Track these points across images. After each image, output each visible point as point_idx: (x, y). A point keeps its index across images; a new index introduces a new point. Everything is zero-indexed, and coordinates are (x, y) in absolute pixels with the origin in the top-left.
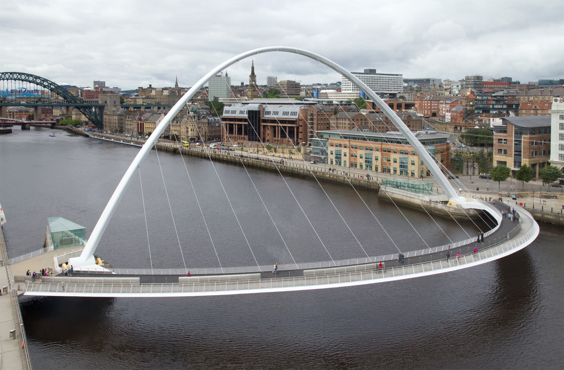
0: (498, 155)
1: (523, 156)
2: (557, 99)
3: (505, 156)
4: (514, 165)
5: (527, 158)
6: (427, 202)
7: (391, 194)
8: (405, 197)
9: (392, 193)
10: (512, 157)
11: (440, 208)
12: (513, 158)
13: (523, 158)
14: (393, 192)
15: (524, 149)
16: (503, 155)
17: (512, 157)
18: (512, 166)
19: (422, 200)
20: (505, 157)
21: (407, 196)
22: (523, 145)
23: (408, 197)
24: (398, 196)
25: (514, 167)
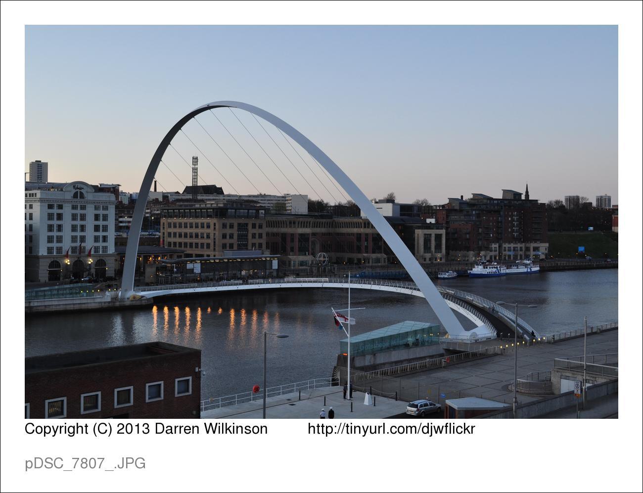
6: (109, 302)
7: (43, 308)
8: (72, 306)
9: (45, 306)
11: (127, 305)
14: (46, 304)
19: (99, 303)
21: (74, 304)
23: (76, 304)
24: (58, 307)
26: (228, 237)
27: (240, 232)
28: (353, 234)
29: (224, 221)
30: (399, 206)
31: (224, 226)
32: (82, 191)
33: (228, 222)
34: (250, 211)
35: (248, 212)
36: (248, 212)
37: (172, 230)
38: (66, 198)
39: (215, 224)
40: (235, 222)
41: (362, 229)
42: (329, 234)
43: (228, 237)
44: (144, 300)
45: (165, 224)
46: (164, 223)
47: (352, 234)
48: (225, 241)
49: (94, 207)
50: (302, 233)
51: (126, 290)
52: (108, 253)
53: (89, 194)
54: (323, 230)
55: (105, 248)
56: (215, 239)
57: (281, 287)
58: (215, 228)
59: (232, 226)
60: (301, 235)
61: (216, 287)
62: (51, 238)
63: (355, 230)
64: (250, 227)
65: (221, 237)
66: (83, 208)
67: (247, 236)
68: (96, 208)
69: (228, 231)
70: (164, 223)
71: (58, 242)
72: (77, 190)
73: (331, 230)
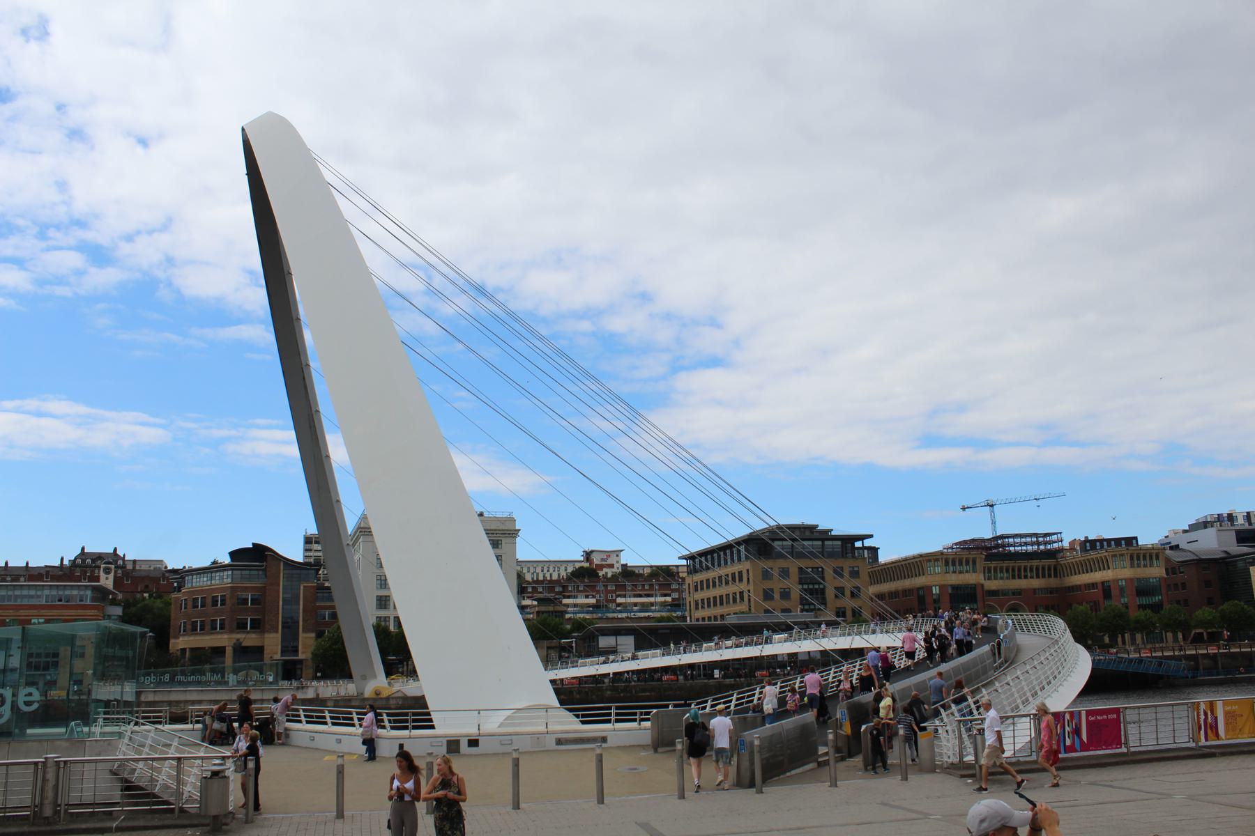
0: (238, 633)
1: (303, 628)
2: (110, 569)
3: (254, 633)
4: (282, 652)
5: (312, 632)
10: (277, 632)
12: (279, 635)
13: (303, 631)
15: (304, 611)
16: (248, 632)
17: (277, 632)
18: (276, 653)
20: (253, 636)
22: (299, 605)
25: (282, 656)
26: (777, 596)
27: (806, 587)
28: (1093, 585)
30: (1234, 533)
31: (766, 575)
33: (774, 566)
34: (827, 543)
35: (823, 544)
36: (823, 544)
37: (699, 595)
39: (748, 570)
40: (793, 565)
41: (1109, 571)
42: (1051, 591)
43: (777, 596)
44: (393, 698)
45: (691, 585)
47: (1093, 584)
50: (957, 583)
51: (364, 678)
54: (1036, 583)
57: (682, 663)
59: (785, 573)
60: (955, 588)
61: (556, 671)
62: (385, 601)
63: (1098, 576)
64: (829, 573)
67: (823, 591)
69: (777, 585)
71: (381, 608)
73: (1053, 582)
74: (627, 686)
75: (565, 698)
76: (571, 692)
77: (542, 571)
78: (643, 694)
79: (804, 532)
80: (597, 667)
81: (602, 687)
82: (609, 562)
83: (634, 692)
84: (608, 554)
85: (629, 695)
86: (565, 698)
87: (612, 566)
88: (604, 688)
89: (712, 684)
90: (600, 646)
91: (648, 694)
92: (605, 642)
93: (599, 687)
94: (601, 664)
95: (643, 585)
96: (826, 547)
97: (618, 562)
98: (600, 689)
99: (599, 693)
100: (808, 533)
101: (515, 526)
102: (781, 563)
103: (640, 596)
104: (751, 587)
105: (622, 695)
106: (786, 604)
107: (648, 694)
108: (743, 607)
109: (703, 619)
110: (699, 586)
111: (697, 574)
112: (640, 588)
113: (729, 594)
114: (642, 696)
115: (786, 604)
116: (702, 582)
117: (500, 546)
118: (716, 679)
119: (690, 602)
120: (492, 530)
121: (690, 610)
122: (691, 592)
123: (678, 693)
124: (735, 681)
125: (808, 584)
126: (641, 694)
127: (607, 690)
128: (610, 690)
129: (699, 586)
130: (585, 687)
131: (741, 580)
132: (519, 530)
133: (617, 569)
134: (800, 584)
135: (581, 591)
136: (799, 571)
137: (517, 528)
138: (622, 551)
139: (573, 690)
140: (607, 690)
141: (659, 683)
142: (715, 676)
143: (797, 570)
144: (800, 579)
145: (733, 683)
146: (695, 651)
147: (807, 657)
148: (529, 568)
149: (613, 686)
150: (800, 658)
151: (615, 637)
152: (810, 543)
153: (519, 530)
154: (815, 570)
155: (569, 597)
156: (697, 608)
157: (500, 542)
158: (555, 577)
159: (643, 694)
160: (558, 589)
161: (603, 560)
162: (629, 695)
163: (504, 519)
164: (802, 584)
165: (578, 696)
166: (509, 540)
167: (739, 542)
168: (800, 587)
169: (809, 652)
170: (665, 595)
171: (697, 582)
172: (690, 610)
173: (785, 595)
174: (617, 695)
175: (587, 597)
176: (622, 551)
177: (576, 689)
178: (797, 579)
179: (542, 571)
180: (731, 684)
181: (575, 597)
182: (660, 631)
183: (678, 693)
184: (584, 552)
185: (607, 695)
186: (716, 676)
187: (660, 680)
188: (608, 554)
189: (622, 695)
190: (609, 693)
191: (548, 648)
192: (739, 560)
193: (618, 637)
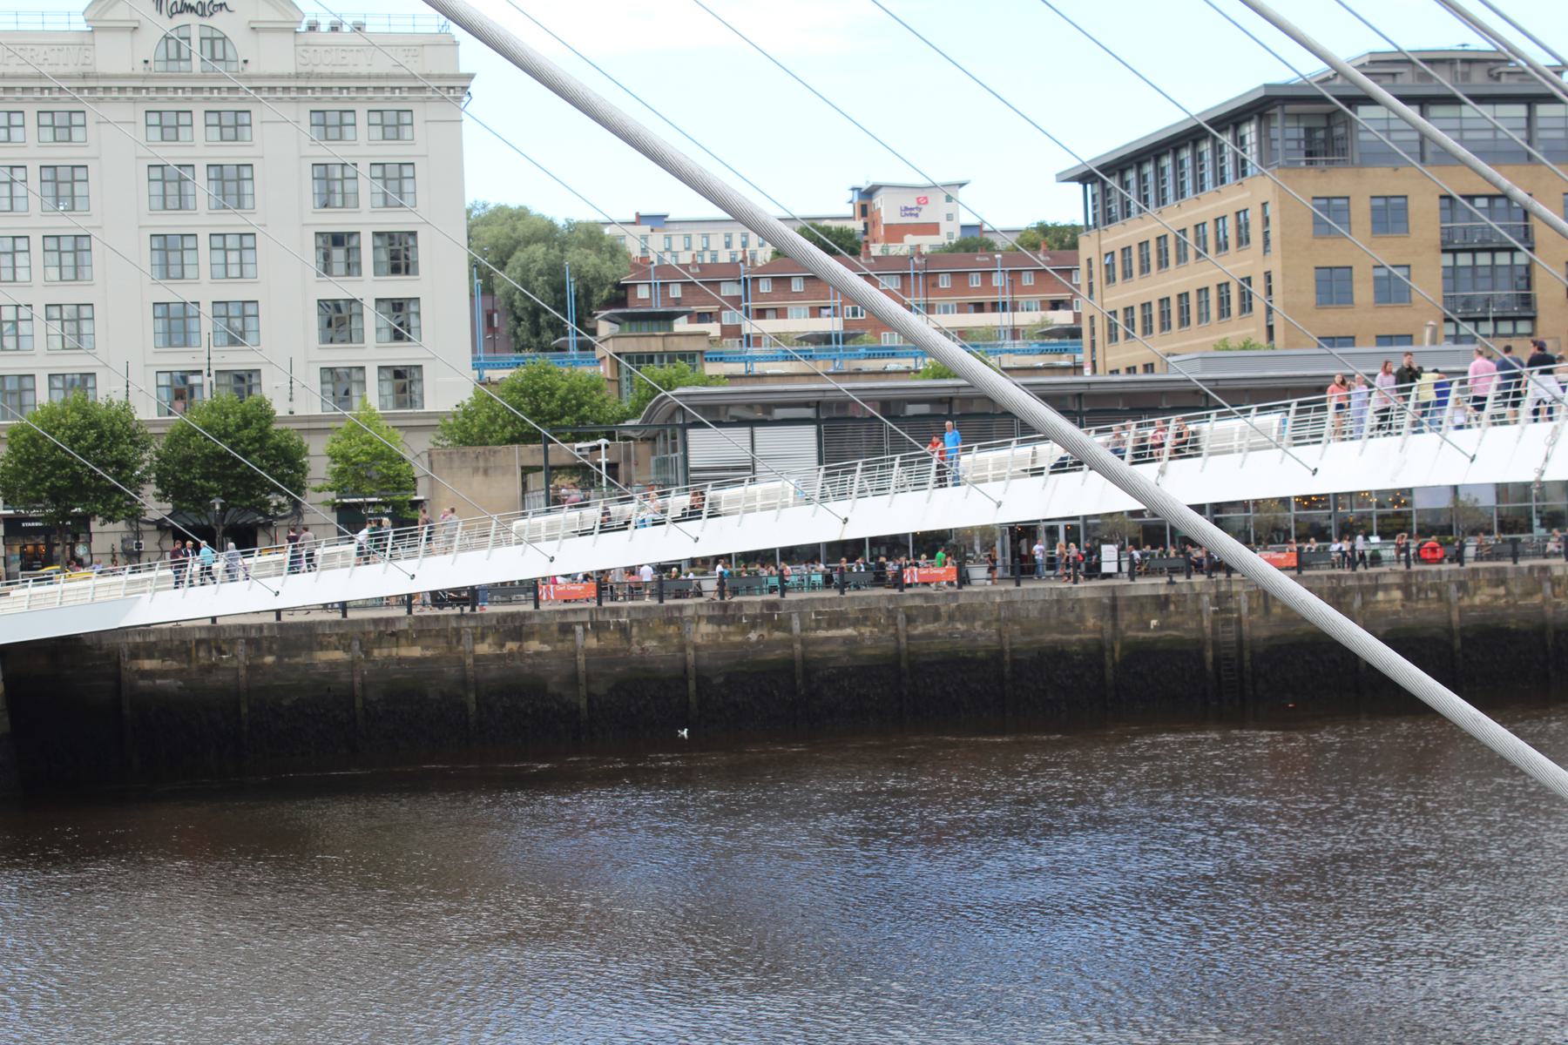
26: (1363, 292)
27: (1464, 260)
29: (1337, 181)
32: (219, 21)
38: (102, 68)
43: (1363, 292)
45: (1095, 263)
46: (1089, 260)
48: (1337, 320)
49: (305, 118)
52: (426, 409)
53: (263, 37)
55: (403, 380)
56: (1269, 310)
57: (851, 533)
58: (1266, 242)
65: (1310, 296)
66: (233, 126)
68: (329, 125)
70: (1089, 260)
72: (182, 19)
74: (773, 606)
75: (547, 648)
76: (566, 629)
77: (728, 245)
78: (831, 633)
79: (1466, 76)
80: (549, 548)
81: (680, 608)
82: (925, 217)
83: (796, 625)
84: (921, 194)
85: (778, 635)
86: (547, 648)
87: (933, 228)
88: (689, 612)
89: (1082, 595)
90: (692, 464)
91: (849, 631)
92: (706, 446)
93: (669, 608)
94: (676, 521)
95: (987, 275)
96: (1540, 123)
97: (949, 217)
98: (672, 618)
99: (672, 630)
100: (1479, 80)
101: (456, 60)
102: (1382, 181)
103: (979, 307)
104: (1275, 264)
105: (753, 636)
106: (1393, 319)
107: (849, 631)
108: (1253, 328)
109: (1131, 370)
110: (1120, 266)
111: (1112, 228)
112: (975, 281)
113: (1187, 294)
114: (828, 639)
115: (1393, 319)
116: (1126, 250)
117: (407, 132)
118: (1109, 576)
119: (1092, 318)
120: (378, 77)
121: (1093, 343)
122: (1096, 287)
123: (961, 626)
124: (1171, 583)
125: (1473, 251)
126: (822, 633)
127: (697, 619)
128: (710, 619)
129: (1120, 266)
130: (616, 611)
131: (1244, 240)
132: (471, 77)
133: (949, 234)
134: (1444, 251)
135: (798, 296)
136: (1442, 209)
137: (464, 69)
138: (961, 185)
139: (571, 619)
140: (697, 619)
141: (896, 592)
142: (1105, 568)
143: (1435, 203)
144: (1447, 234)
145: (1162, 592)
146: (902, 488)
147: (1444, 502)
148: (689, 237)
149: (725, 607)
150: (1420, 503)
151: (746, 431)
152: (1486, 110)
153: (471, 77)
154: (1500, 203)
155: (761, 314)
156: (1113, 337)
157: (406, 118)
158: (724, 258)
159: (831, 633)
160: (729, 290)
161: (907, 211)
162: (778, 635)
163: (419, 41)
164: (1454, 252)
165: (592, 643)
166: (436, 111)
167: (1232, 120)
168: (1447, 260)
169: (1455, 488)
170: (1055, 305)
171: (1113, 253)
172: (1093, 343)
173: (1391, 290)
174: (738, 639)
175: (816, 312)
176: (961, 185)
177: (585, 617)
178: (1435, 236)
179: (728, 245)
180: (1158, 597)
181: (781, 313)
182: (912, 410)
183: (961, 626)
184: (853, 189)
185: (699, 640)
186: (1108, 566)
187: (898, 582)
188: (923, 193)
189: (753, 636)
190: (705, 628)
191: (526, 470)
192: (1241, 168)
193: (759, 431)
